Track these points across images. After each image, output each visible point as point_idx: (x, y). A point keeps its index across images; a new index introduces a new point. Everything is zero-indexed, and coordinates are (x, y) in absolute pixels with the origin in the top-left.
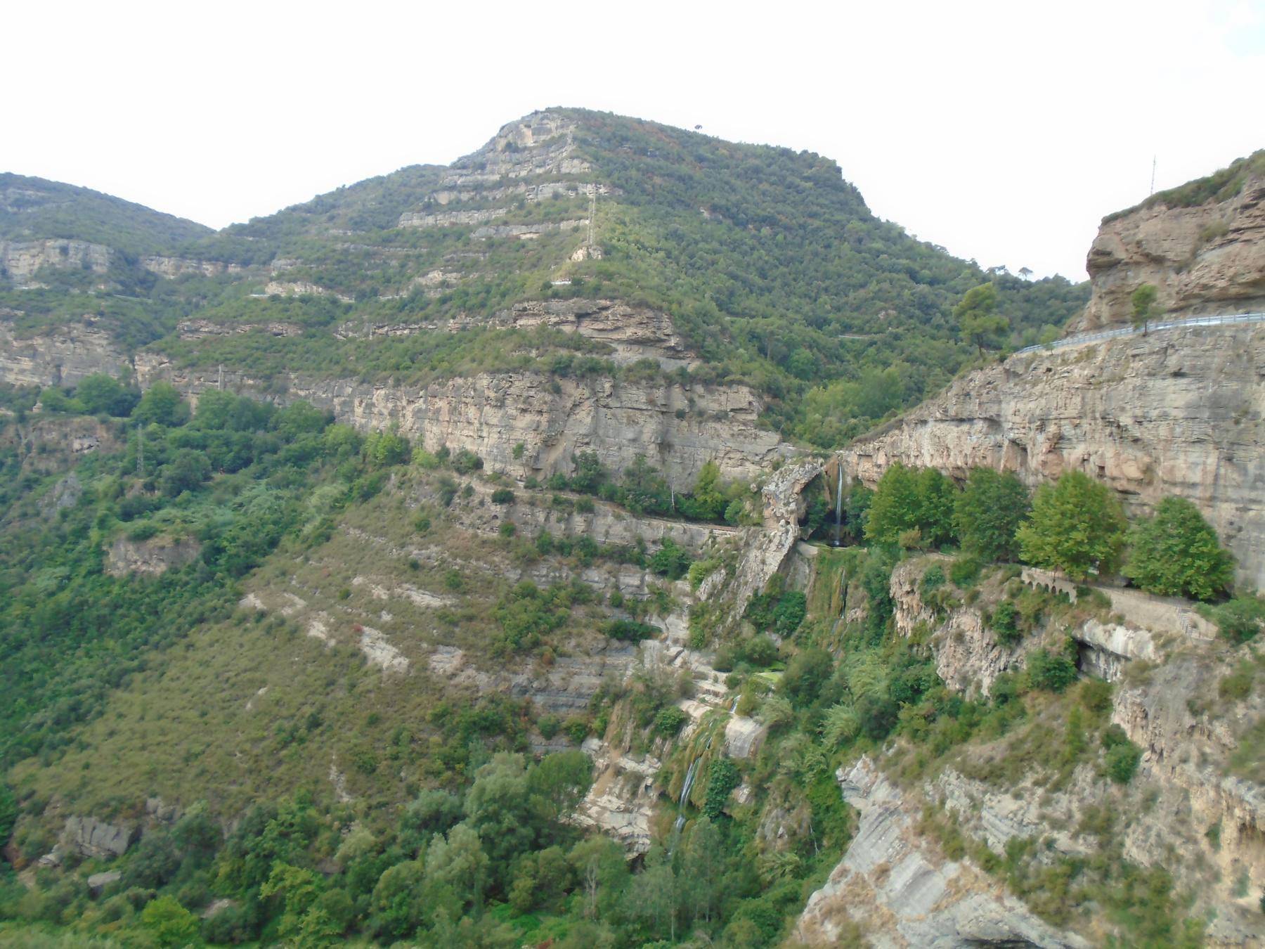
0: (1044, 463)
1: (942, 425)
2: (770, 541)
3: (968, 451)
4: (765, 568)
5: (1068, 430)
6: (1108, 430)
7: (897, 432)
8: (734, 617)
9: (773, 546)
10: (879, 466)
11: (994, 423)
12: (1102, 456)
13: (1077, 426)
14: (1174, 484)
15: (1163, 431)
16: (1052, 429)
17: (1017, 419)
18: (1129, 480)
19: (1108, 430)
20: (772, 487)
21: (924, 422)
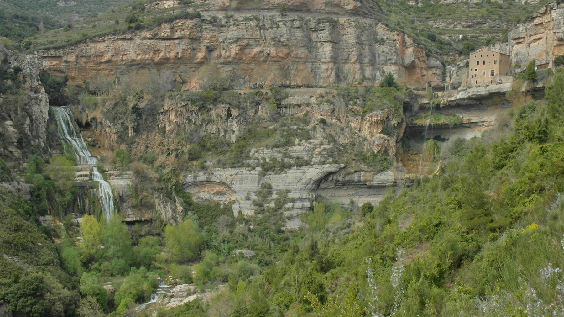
0: (237, 54)
1: (152, 41)
2: (41, 101)
3: (181, 51)
4: (44, 116)
5: (252, 42)
6: (273, 43)
7: (84, 45)
8: (43, 142)
9: (43, 103)
10: (66, 62)
11: (194, 40)
12: (270, 51)
13: (256, 41)
14: (296, 58)
15: (295, 43)
16: (245, 42)
17: (213, 39)
18: (280, 57)
19: (273, 43)
20: (29, 71)
21: (131, 39)
